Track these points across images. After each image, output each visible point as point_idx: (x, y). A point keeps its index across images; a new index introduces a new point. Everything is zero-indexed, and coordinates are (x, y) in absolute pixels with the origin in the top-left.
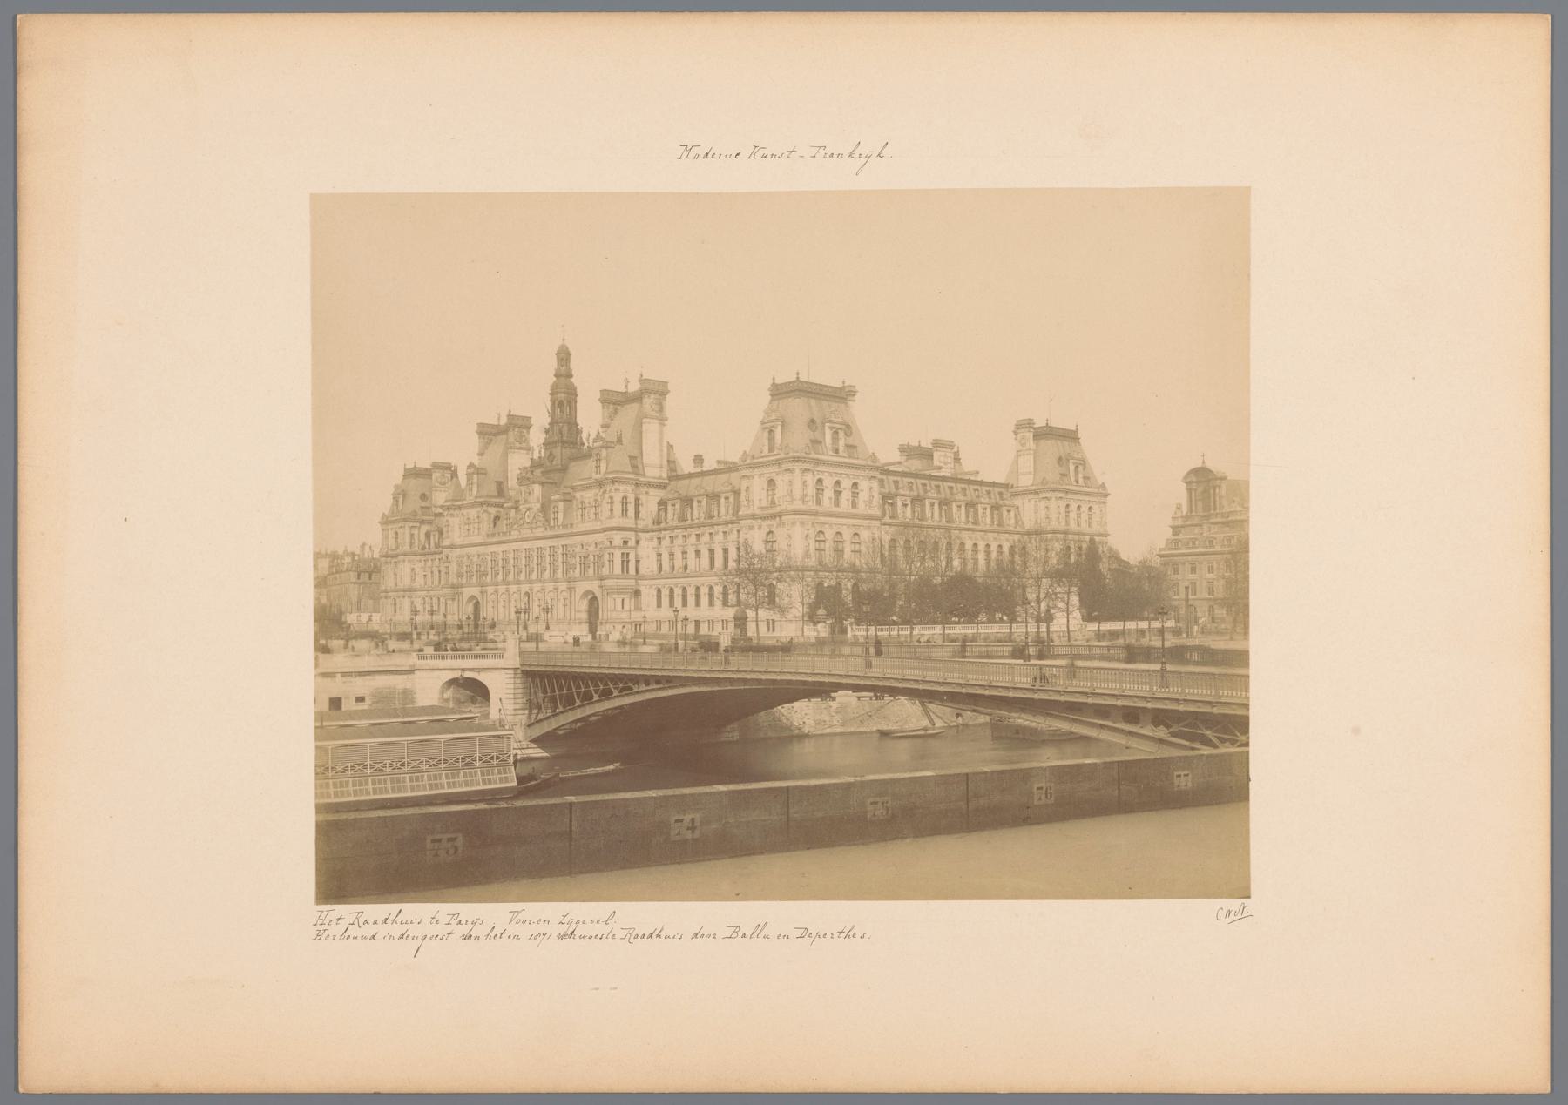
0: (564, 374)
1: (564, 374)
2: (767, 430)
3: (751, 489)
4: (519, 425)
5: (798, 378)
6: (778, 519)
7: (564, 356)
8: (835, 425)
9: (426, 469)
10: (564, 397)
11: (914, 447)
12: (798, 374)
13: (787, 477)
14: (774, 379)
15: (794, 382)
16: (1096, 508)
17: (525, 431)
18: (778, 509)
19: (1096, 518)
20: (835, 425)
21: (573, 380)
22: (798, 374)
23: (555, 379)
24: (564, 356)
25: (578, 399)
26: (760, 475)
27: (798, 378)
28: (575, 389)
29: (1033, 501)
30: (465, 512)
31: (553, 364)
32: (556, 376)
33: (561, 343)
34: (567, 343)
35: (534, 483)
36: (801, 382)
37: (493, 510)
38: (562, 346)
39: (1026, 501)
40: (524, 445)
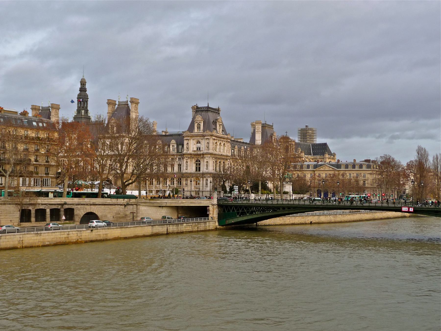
0: (83, 89)
1: (83, 89)
2: (197, 123)
3: (189, 144)
5: (208, 106)
6: (202, 156)
7: (83, 83)
12: (208, 104)
13: (207, 141)
15: (207, 107)
17: (57, 110)
18: (202, 152)
21: (86, 92)
22: (208, 104)
23: (80, 92)
24: (83, 83)
25: (89, 100)
26: (193, 140)
27: (208, 106)
28: (87, 96)
31: (79, 86)
33: (82, 77)
34: (85, 78)
40: (57, 116)
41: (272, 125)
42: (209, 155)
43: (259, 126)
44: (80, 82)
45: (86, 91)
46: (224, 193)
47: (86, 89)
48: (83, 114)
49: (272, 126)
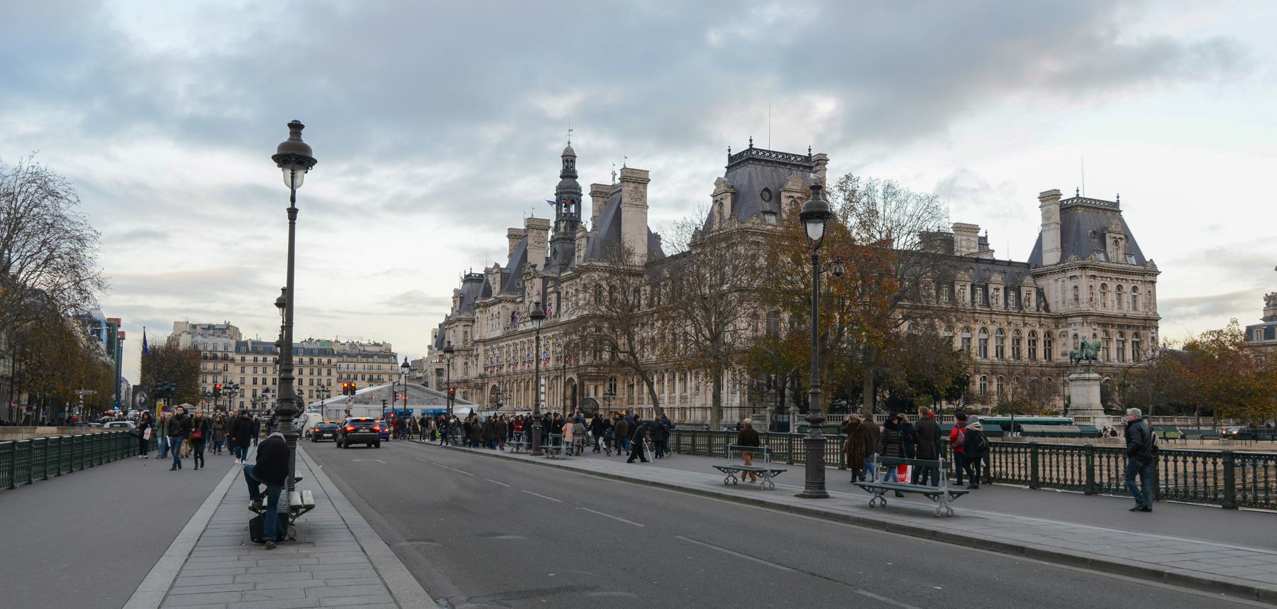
0: (569, 173)
1: (569, 173)
4: (535, 225)
5: (751, 145)
8: (793, 194)
9: (481, 275)
10: (568, 193)
11: (933, 233)
12: (751, 140)
14: (729, 150)
15: (748, 150)
16: (1141, 288)
17: (543, 232)
19: (1141, 300)
20: (793, 194)
22: (751, 140)
24: (569, 159)
27: (751, 145)
28: (581, 188)
29: (1060, 281)
30: (491, 308)
31: (558, 169)
32: (561, 177)
35: (535, 277)
36: (755, 149)
37: (511, 307)
38: (566, 150)
39: (1052, 281)
41: (1115, 200)
42: (1080, 318)
43: (1051, 207)
44: (562, 157)
45: (577, 177)
46: (801, 413)
47: (574, 171)
48: (562, 230)
49: (1117, 204)
